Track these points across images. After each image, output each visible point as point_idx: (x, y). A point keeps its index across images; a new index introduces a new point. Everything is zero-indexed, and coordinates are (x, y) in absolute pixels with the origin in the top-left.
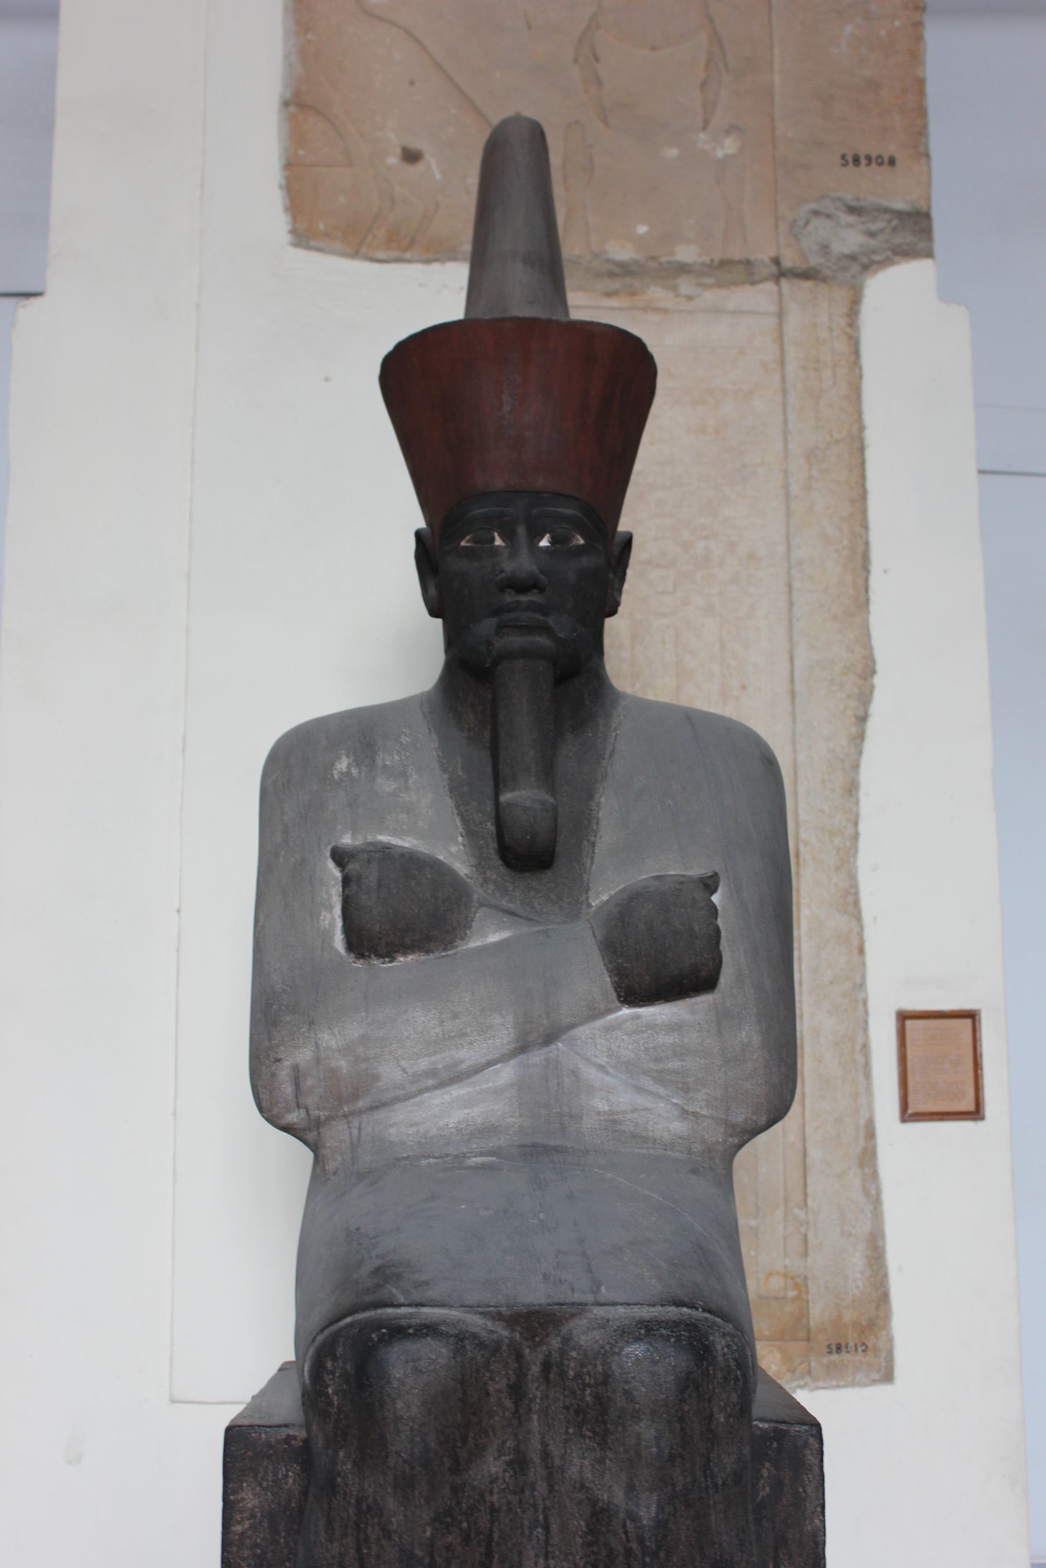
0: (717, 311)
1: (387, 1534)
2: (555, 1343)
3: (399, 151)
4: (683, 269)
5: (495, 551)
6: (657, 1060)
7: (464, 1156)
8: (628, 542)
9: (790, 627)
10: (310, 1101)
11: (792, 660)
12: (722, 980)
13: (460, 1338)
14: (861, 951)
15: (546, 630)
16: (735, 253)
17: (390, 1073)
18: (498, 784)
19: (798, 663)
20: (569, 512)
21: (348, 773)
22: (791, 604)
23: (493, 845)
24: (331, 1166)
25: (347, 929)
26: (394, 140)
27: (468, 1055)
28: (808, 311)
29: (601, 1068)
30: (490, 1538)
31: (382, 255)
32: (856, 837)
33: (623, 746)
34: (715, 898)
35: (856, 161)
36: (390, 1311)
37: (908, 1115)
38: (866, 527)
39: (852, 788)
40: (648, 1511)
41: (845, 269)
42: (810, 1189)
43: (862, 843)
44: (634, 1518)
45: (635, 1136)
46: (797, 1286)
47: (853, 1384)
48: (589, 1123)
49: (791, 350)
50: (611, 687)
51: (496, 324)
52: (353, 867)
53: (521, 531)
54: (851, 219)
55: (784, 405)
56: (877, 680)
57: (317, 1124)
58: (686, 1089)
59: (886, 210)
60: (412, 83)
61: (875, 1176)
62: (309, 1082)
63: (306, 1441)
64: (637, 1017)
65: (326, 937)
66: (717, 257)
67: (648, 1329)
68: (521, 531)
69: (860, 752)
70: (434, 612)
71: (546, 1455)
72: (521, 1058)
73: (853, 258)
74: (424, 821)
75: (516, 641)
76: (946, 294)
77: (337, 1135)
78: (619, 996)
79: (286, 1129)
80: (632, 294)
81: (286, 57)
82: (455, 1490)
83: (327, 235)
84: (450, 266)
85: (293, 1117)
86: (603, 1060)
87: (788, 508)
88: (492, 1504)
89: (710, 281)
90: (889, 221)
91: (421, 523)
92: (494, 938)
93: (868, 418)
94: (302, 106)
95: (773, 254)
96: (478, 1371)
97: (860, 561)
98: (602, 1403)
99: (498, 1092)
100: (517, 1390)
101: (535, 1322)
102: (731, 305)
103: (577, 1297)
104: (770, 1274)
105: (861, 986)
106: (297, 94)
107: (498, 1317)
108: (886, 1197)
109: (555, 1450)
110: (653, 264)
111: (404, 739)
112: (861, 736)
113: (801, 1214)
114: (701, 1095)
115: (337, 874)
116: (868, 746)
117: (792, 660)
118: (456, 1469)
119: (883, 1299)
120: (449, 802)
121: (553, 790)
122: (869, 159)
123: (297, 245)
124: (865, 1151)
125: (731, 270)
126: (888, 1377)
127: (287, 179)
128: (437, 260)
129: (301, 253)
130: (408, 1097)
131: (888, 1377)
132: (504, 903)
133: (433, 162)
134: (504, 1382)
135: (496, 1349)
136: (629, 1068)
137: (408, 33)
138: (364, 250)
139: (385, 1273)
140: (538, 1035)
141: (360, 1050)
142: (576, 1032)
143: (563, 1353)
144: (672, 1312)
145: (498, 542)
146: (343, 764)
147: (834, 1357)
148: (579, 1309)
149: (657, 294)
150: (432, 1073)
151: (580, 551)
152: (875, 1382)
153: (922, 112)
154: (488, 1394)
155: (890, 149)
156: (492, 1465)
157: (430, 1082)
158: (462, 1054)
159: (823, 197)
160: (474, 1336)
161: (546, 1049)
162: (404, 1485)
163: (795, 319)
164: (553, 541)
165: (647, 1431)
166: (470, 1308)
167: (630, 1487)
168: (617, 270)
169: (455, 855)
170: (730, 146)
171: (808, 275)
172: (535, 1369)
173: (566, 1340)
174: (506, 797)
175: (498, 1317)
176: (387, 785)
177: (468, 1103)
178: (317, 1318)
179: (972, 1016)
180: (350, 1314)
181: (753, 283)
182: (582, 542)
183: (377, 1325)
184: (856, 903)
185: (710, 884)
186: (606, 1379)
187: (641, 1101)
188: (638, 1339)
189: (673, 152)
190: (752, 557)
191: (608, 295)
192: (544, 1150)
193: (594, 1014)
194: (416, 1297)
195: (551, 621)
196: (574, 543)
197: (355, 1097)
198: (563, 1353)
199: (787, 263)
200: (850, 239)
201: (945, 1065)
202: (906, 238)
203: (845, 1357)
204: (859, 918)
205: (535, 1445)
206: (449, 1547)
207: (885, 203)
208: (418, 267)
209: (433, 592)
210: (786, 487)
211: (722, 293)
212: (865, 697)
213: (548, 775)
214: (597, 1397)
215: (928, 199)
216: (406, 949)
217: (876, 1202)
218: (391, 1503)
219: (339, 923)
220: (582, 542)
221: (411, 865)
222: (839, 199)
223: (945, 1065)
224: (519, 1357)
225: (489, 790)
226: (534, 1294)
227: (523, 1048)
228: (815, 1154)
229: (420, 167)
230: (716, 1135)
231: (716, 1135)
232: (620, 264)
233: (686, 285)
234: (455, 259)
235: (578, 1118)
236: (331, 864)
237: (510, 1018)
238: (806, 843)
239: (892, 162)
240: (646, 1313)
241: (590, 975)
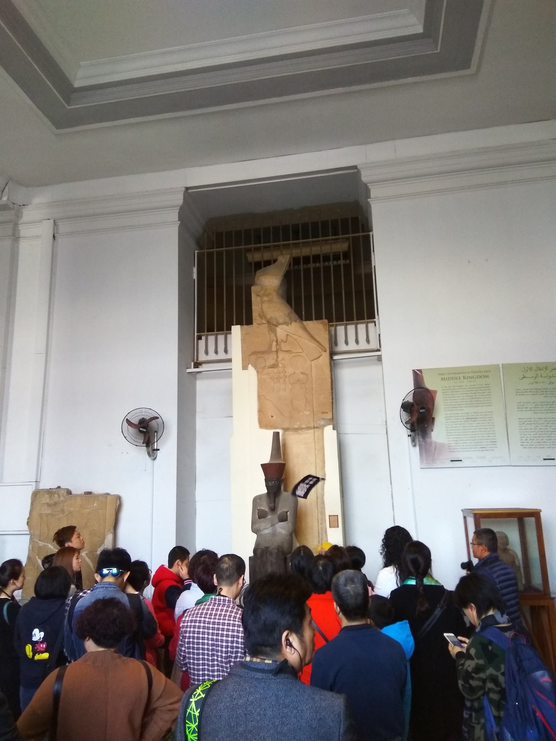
125: (309, 428)
140: (273, 525)
149: (300, 431)
170: (308, 413)
241: (276, 520)
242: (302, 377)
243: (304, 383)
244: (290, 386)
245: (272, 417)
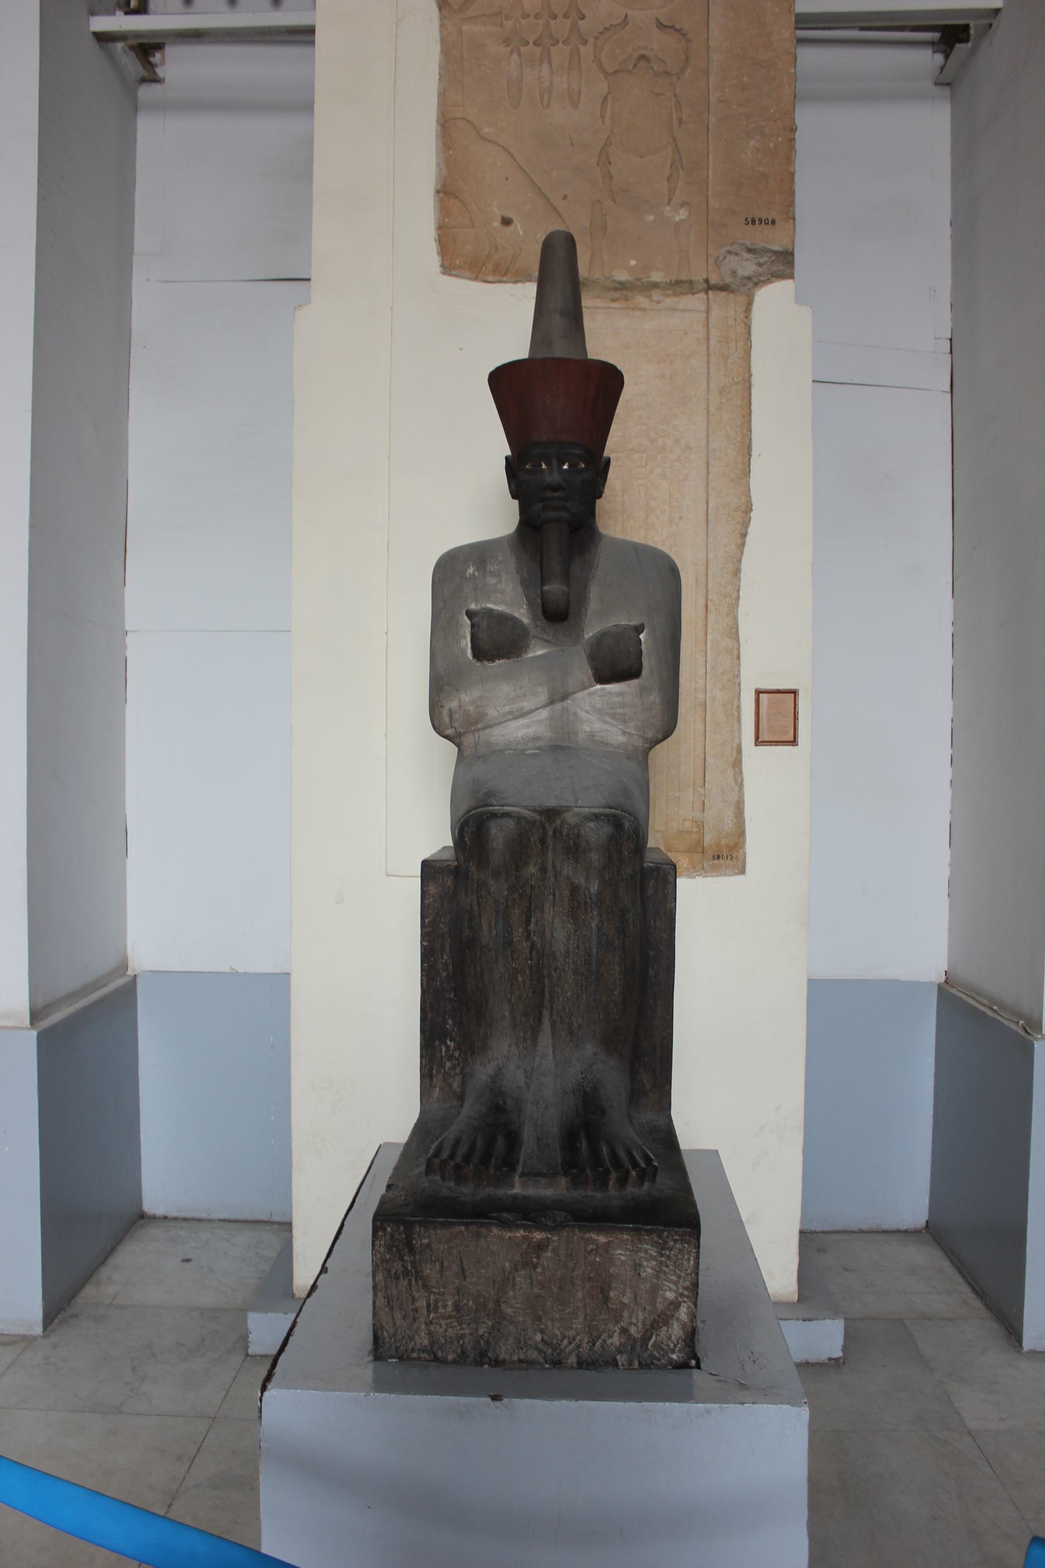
0: (674, 310)
1: (489, 893)
2: (559, 822)
4: (655, 285)
5: (542, 471)
6: (613, 708)
7: (525, 750)
8: (608, 462)
9: (707, 485)
10: (456, 724)
11: (707, 503)
12: (643, 673)
13: (519, 819)
14: (738, 657)
15: (566, 509)
16: (685, 279)
17: (492, 712)
18: (544, 581)
19: (710, 505)
20: (577, 452)
21: (474, 574)
22: (708, 473)
23: (540, 609)
24: (466, 753)
25: (473, 648)
26: (497, 213)
27: (527, 705)
28: (724, 309)
29: (587, 712)
30: (531, 898)
31: (491, 279)
32: (738, 598)
33: (603, 560)
34: (642, 636)
35: (753, 222)
36: (491, 808)
37: (758, 742)
38: (751, 431)
39: (737, 572)
40: (594, 888)
41: (745, 285)
42: (707, 779)
43: (740, 601)
44: (588, 889)
45: (601, 742)
46: (698, 826)
47: (725, 875)
48: (581, 736)
49: (712, 331)
50: (599, 533)
51: (544, 361)
52: (476, 620)
53: (555, 462)
54: (749, 256)
55: (708, 363)
56: (752, 514)
57: (460, 735)
58: (625, 722)
59: (769, 251)
60: (507, 179)
61: (741, 772)
62: (457, 716)
63: (456, 867)
64: (604, 689)
65: (464, 652)
66: (674, 279)
67: (596, 817)
68: (555, 462)
69: (742, 553)
70: (514, 497)
71: (554, 867)
72: (551, 707)
73: (749, 278)
74: (507, 598)
75: (551, 514)
76: (799, 300)
77: (469, 740)
79: (446, 737)
80: (627, 300)
81: (438, 165)
82: (516, 878)
83: (461, 267)
84: (527, 284)
85: (449, 732)
86: (588, 708)
87: (708, 419)
89: (670, 292)
90: (770, 257)
91: (509, 453)
92: (539, 653)
93: (754, 370)
94: (446, 193)
95: (705, 277)
97: (746, 450)
98: (577, 846)
99: (540, 722)
100: (543, 841)
101: (551, 814)
102: (680, 307)
103: (568, 804)
104: (685, 820)
105: (738, 676)
106: (444, 185)
107: (535, 811)
108: (745, 783)
109: (558, 865)
110: (639, 283)
111: (500, 558)
112: (743, 544)
113: (702, 791)
114: (632, 724)
115: (469, 622)
116: (747, 550)
117: (707, 503)
118: (517, 869)
119: (742, 833)
120: (520, 589)
121: (568, 584)
122: (760, 221)
123: (444, 273)
124: (736, 760)
125: (681, 286)
126: (742, 871)
127: (439, 235)
128: (520, 281)
129: (447, 278)
130: (501, 723)
131: (742, 871)
132: (545, 637)
135: (534, 823)
136: (600, 712)
137: (505, 149)
138: (481, 275)
139: (489, 794)
140: (559, 696)
141: (479, 703)
142: (576, 695)
143: (562, 826)
144: (607, 811)
145: (544, 466)
146: (471, 570)
147: (716, 861)
148: (568, 809)
149: (640, 300)
150: (511, 713)
151: (582, 471)
152: (736, 874)
153: (792, 193)
155: (773, 215)
156: (532, 869)
158: (524, 704)
159: (734, 243)
160: (525, 818)
162: (496, 875)
163: (716, 314)
164: (569, 466)
165: (595, 858)
166: (524, 807)
167: (587, 878)
168: (618, 286)
169: (522, 614)
170: (683, 214)
171: (724, 288)
172: (551, 833)
173: (563, 821)
174: (546, 588)
175: (535, 811)
176: (491, 581)
177: (528, 726)
178: (461, 813)
179: (794, 692)
180: (475, 809)
181: (693, 294)
183: (486, 813)
184: (737, 633)
185: (639, 629)
186: (578, 836)
187: (605, 727)
188: (592, 820)
189: (652, 217)
190: (688, 447)
191: (614, 300)
192: (561, 747)
193: (584, 688)
194: (502, 803)
195: (568, 505)
197: (477, 722)
198: (562, 826)
199: (713, 282)
200: (748, 267)
201: (779, 718)
202: (778, 267)
203: (721, 861)
204: (738, 641)
205: (550, 863)
206: (514, 899)
207: (769, 247)
208: (511, 285)
209: (514, 487)
210: (708, 408)
211: (676, 299)
212: (746, 523)
213: (566, 577)
214: (574, 843)
215: (793, 244)
216: (500, 657)
217: (741, 786)
218: (491, 882)
219: (469, 645)
221: (503, 619)
222: (743, 244)
223: (779, 718)
224: (544, 827)
225: (539, 583)
226: (551, 802)
227: (551, 702)
228: (710, 760)
229: (511, 228)
230: (639, 743)
231: (639, 743)
232: (621, 283)
233: (656, 295)
234: (530, 281)
235: (577, 734)
236: (466, 618)
237: (546, 689)
238: (712, 601)
239: (773, 222)
240: (596, 811)
241: (582, 670)
242: (659, 43)
243: (667, 73)
244: (603, 86)
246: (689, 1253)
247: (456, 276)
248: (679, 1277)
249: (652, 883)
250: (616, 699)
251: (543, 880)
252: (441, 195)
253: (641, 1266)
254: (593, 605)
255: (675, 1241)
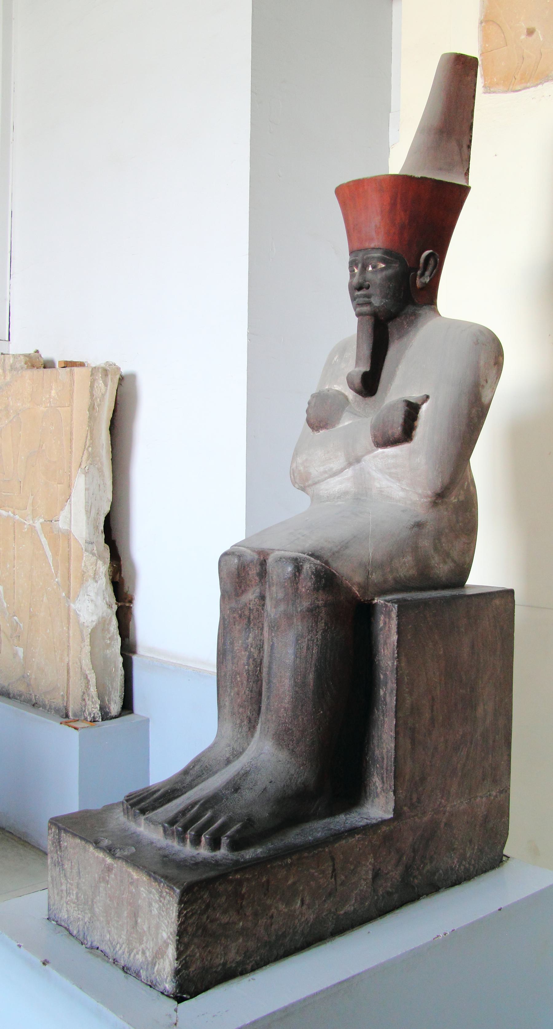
3: (525, 31)
27: (336, 465)
30: (249, 618)
58: (399, 480)
78: (375, 445)
88: (250, 608)
92: (346, 423)
96: (244, 567)
130: (323, 481)
133: (539, 32)
134: (255, 572)
138: (511, 87)
150: (325, 472)
151: (382, 270)
154: (248, 574)
157: (326, 475)
161: (359, 464)
164: (373, 268)
182: (383, 266)
196: (379, 267)
206: (234, 618)
220: (383, 266)
227: (350, 464)
245: (530, 32)
246: (173, 905)
247: (494, 92)
248: (168, 922)
249: (382, 617)
250: (391, 461)
251: (263, 605)
252: (483, 24)
253: (151, 904)
254: (397, 381)
255: (167, 893)
